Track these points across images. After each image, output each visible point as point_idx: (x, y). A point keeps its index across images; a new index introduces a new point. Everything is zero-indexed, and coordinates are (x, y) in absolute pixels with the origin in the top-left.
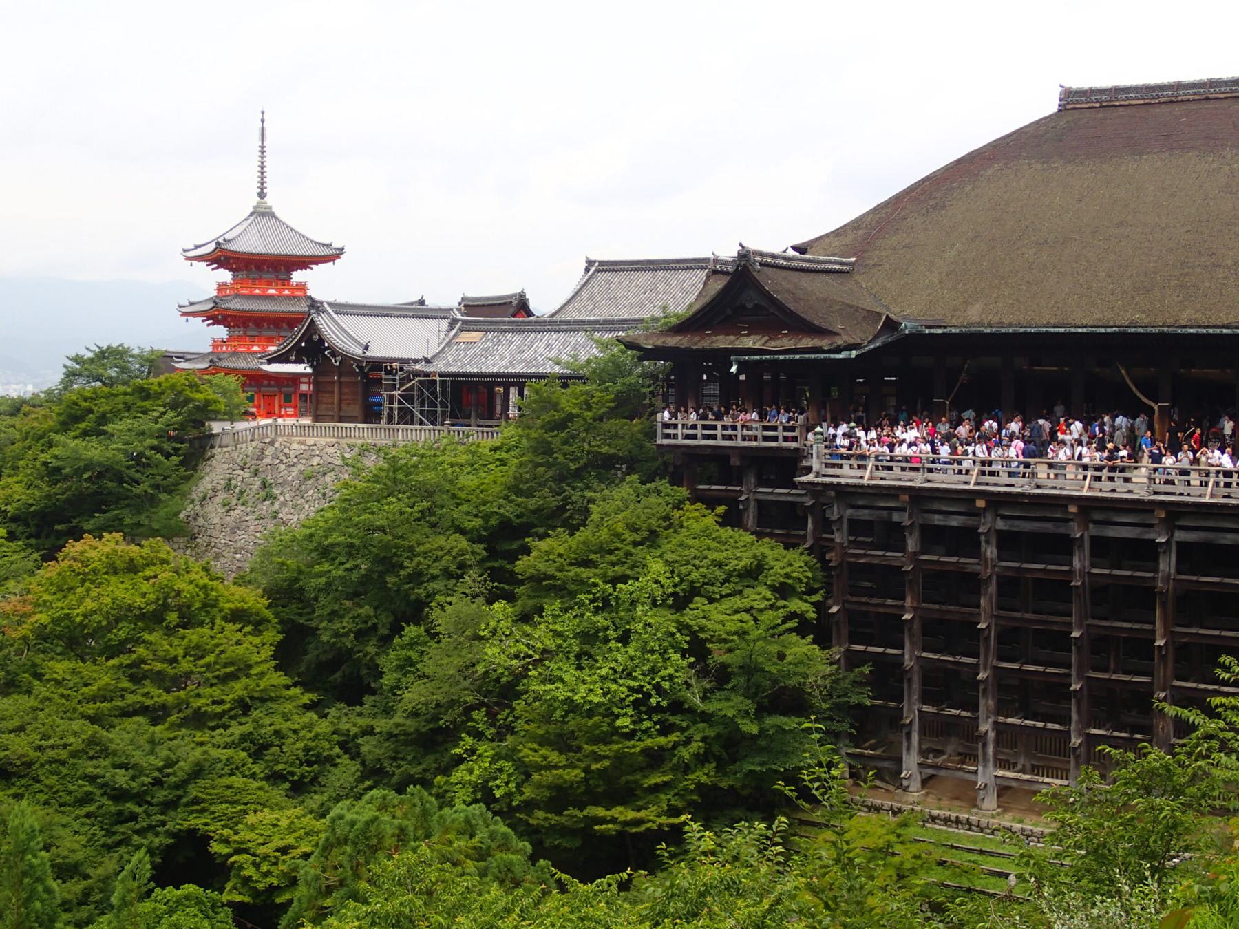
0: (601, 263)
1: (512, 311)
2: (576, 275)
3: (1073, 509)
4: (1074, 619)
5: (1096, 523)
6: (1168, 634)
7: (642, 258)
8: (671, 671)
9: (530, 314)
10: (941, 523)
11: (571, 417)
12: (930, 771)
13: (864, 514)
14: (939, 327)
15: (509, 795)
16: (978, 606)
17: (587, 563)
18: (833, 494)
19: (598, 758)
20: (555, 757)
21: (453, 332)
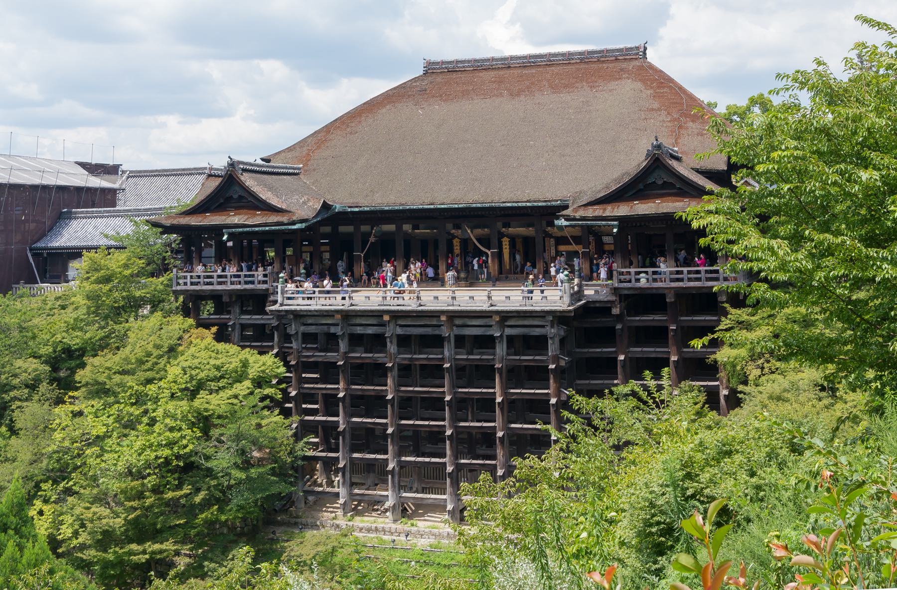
3: (443, 318)
5: (458, 326)
7: (183, 167)
10: (362, 332)
13: (312, 329)
18: (292, 317)
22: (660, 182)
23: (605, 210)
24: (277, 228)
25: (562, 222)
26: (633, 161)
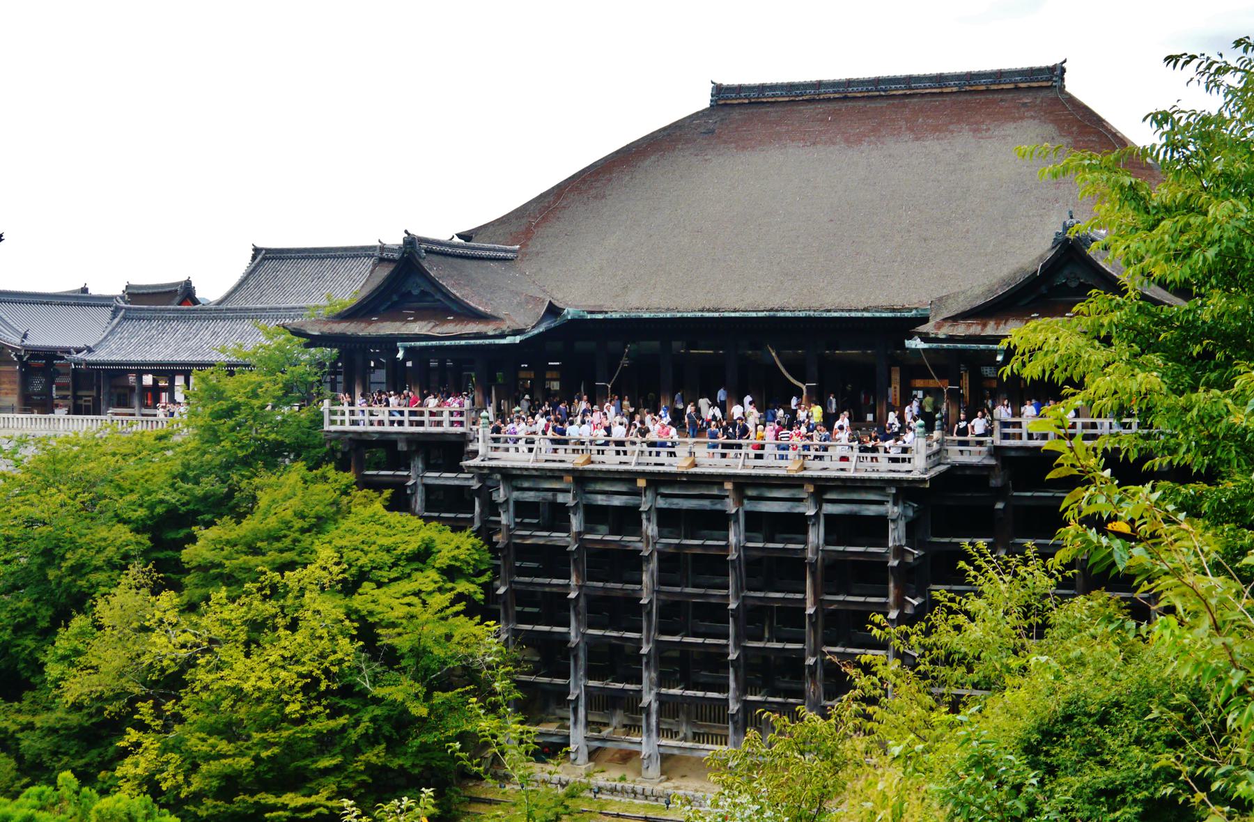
0: (268, 251)
1: (178, 299)
2: (243, 262)
4: (731, 591)
6: (818, 601)
8: (340, 655)
9: (196, 302)
10: (605, 503)
11: (238, 406)
12: (597, 744)
13: (530, 496)
14: (601, 312)
15: (178, 787)
16: (640, 583)
17: (256, 552)
18: (499, 477)
19: (267, 745)
20: (224, 746)
21: (116, 320)
22: (1073, 284)
23: (985, 326)
24: (478, 342)
25: (916, 344)
26: (1030, 251)
